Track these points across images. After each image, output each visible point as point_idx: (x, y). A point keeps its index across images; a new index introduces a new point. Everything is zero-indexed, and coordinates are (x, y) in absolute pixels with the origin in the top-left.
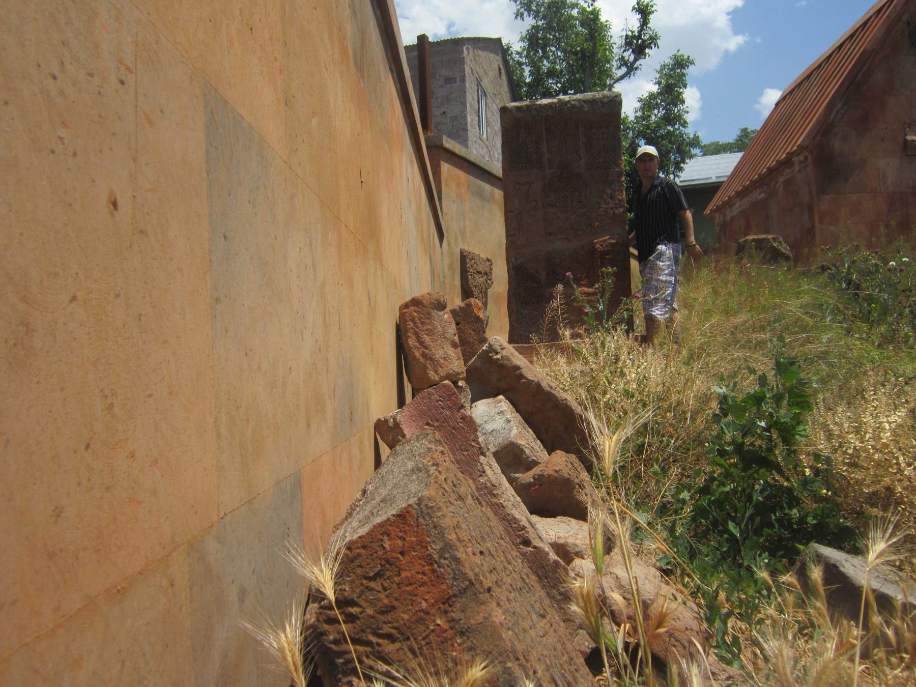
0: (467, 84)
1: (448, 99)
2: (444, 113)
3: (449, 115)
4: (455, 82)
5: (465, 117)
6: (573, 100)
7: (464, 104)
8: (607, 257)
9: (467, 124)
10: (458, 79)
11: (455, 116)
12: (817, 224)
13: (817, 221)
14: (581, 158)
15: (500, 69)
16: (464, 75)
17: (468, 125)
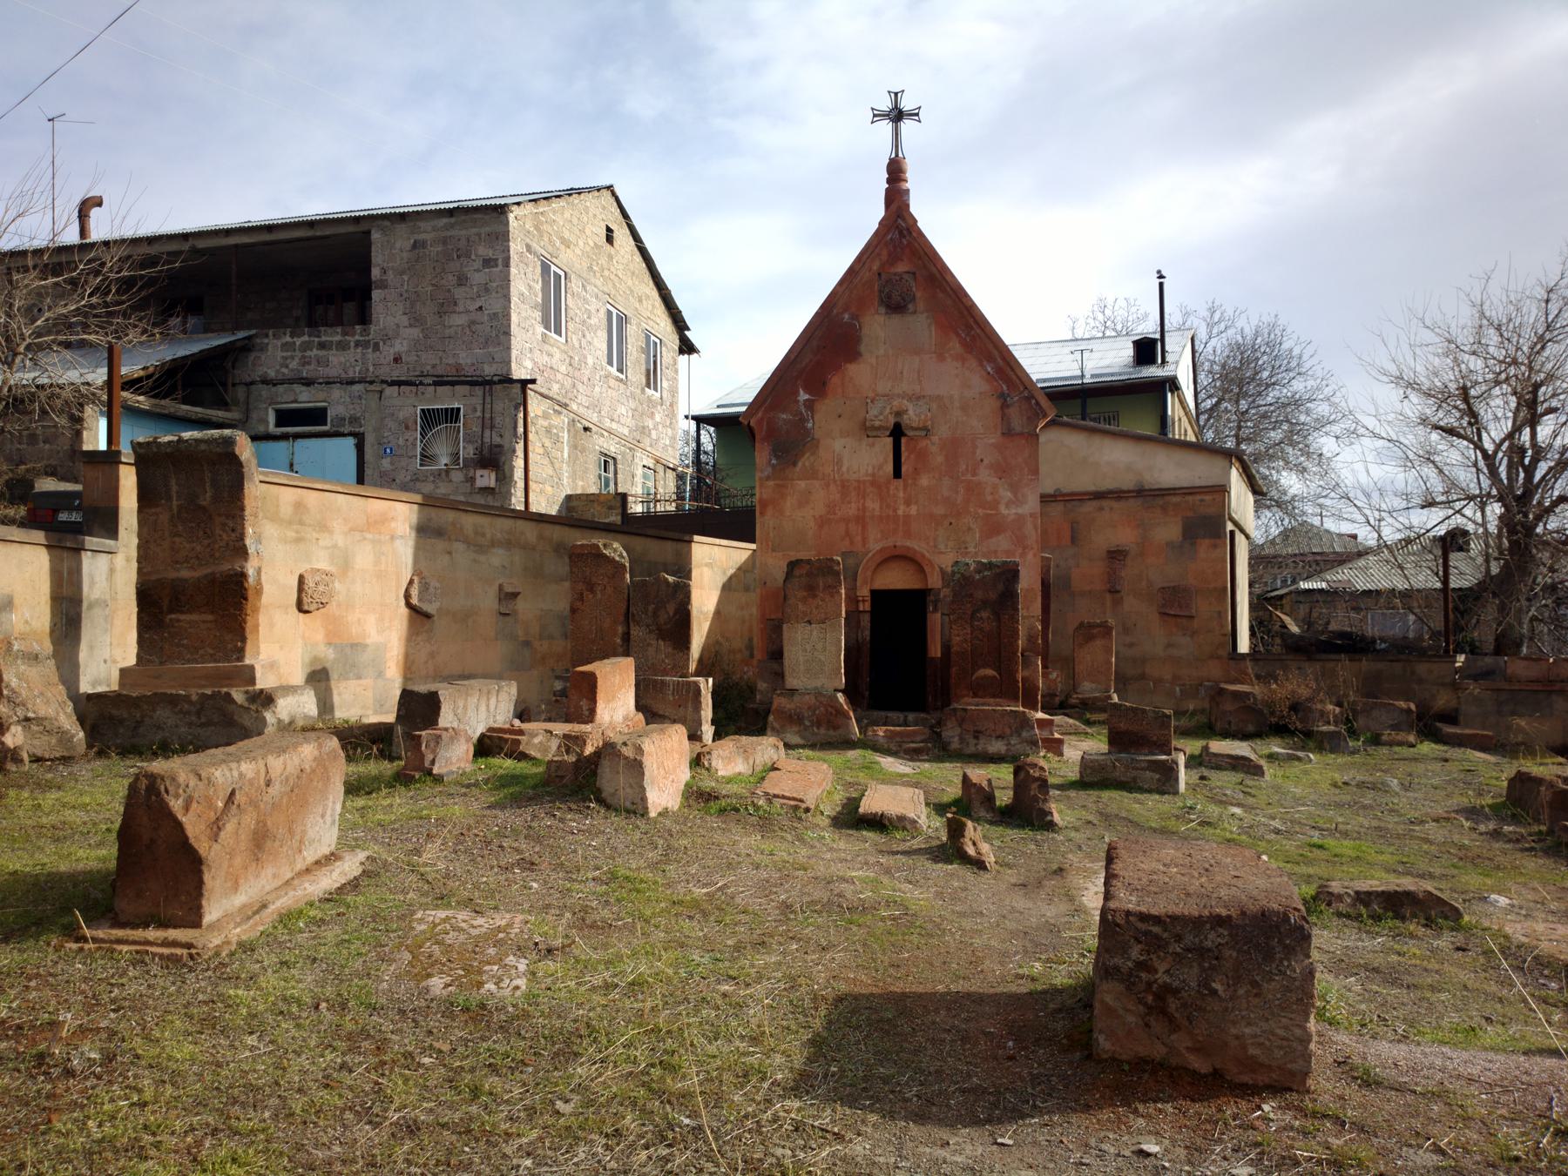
0: (513, 270)
2: (481, 308)
4: (497, 266)
5: (507, 316)
16: (509, 258)
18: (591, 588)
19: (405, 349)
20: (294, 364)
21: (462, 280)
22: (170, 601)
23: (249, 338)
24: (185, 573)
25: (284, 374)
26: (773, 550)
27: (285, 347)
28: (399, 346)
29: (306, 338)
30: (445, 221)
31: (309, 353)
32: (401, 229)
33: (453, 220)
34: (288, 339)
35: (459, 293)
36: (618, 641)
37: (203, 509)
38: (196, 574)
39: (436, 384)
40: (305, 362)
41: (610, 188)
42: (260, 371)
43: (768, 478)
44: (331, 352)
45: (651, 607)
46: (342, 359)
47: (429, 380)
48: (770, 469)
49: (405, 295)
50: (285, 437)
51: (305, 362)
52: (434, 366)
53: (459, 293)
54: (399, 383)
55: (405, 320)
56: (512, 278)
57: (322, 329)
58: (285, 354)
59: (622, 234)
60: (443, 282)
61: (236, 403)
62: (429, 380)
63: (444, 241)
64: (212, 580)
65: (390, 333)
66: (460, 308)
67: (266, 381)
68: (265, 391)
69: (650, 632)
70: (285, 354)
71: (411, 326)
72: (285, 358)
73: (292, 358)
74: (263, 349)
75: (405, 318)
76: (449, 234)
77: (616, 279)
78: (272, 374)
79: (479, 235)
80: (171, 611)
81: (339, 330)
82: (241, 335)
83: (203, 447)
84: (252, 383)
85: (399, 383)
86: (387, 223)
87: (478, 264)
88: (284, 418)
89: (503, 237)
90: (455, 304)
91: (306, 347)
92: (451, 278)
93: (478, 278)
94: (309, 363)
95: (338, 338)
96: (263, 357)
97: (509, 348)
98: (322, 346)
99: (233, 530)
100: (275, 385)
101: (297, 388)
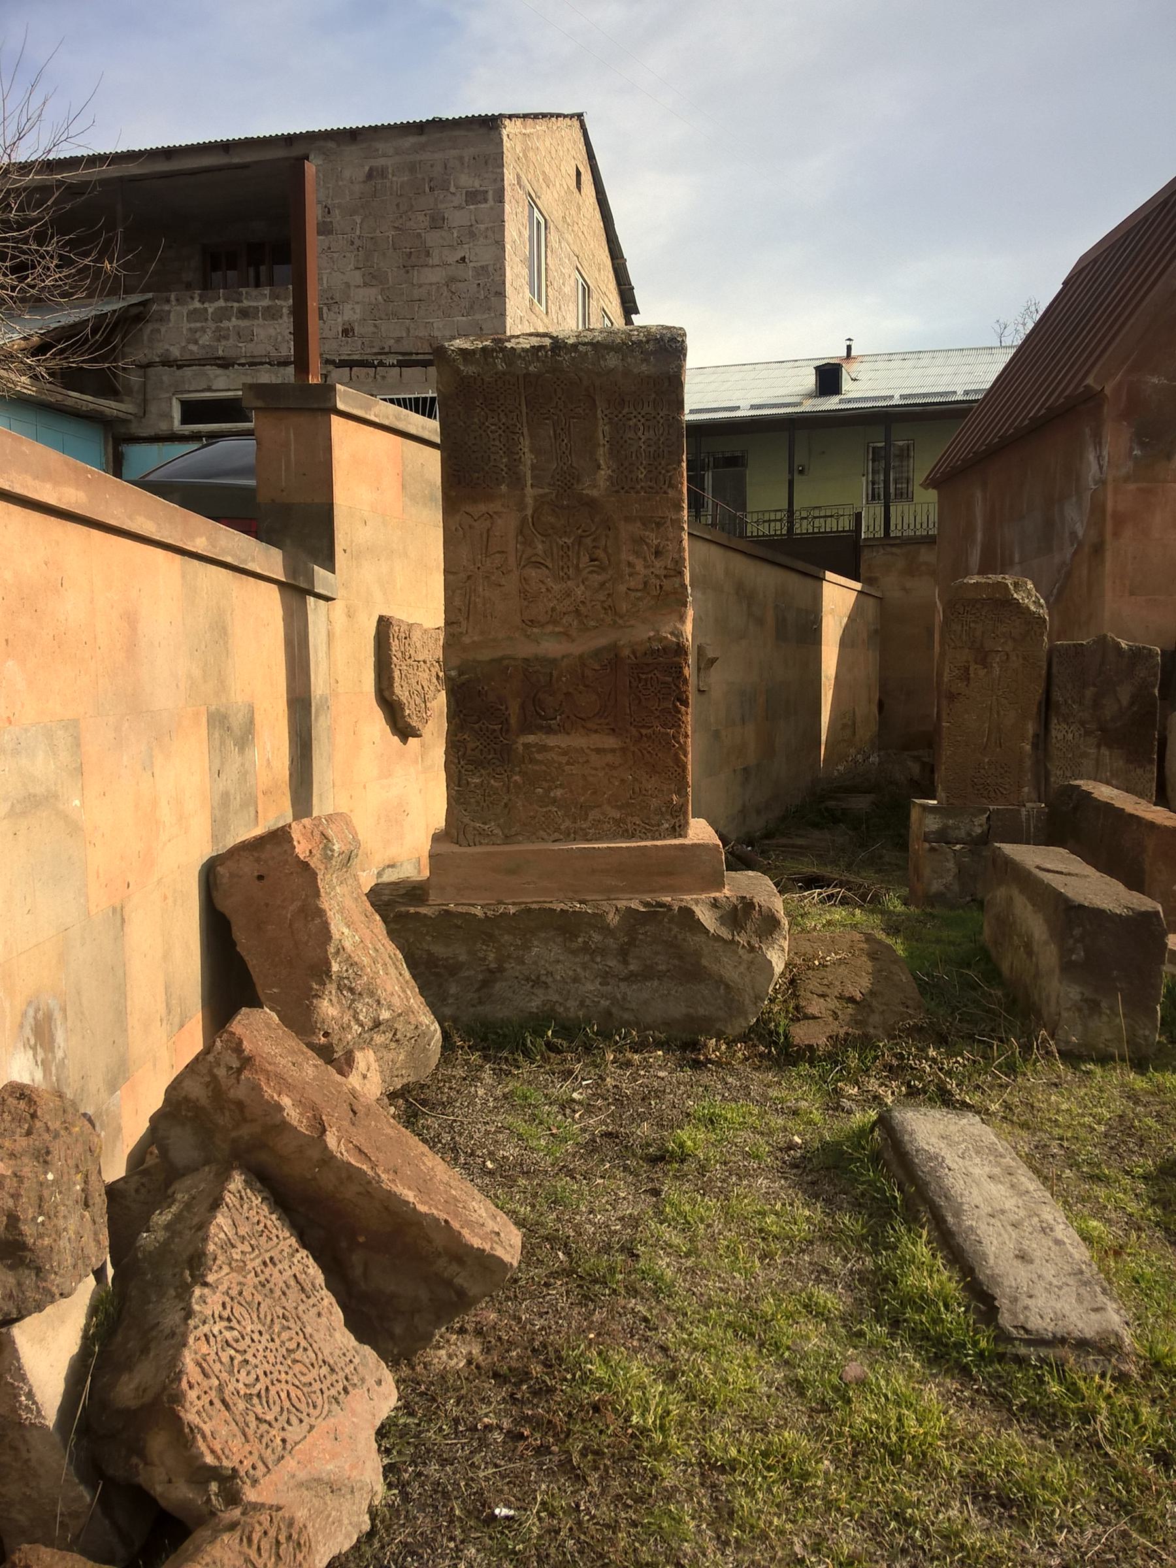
0: (507, 207)
1: (471, 233)
2: (463, 259)
3: (472, 264)
4: (486, 200)
6: (585, 344)
7: (500, 244)
8: (644, 676)
9: (504, 283)
10: (490, 195)
11: (482, 267)
12: (1108, 537)
13: (1109, 527)
14: (599, 467)
15: (578, 174)
16: (503, 189)
17: (507, 285)
18: (983, 657)
19: (357, 316)
20: (205, 339)
21: (437, 222)
22: (523, 707)
23: (143, 304)
24: (551, 647)
25: (192, 352)
26: (1132, 594)
27: (193, 315)
28: (350, 313)
29: (221, 303)
30: (411, 140)
31: (225, 324)
32: (352, 152)
33: (423, 139)
34: (197, 305)
35: (433, 239)
36: (1028, 747)
37: (591, 504)
38: (577, 648)
39: (401, 364)
40: (221, 336)
41: (580, 116)
42: (160, 348)
43: (1127, 479)
44: (256, 322)
45: (1090, 692)
46: (272, 332)
47: (392, 360)
48: (1130, 464)
49: (357, 243)
50: (195, 437)
51: (221, 336)
52: (399, 340)
53: (433, 239)
54: (350, 364)
55: (357, 277)
56: (506, 218)
57: (244, 290)
58: (192, 325)
59: (587, 177)
60: (412, 223)
61: (129, 392)
62: (392, 360)
63: (412, 168)
64: (612, 659)
65: (337, 298)
66: (435, 260)
67: (167, 363)
68: (166, 375)
69: (1088, 733)
70: (192, 325)
71: (366, 285)
72: (193, 331)
73: (203, 330)
74: (163, 318)
75: (358, 273)
76: (418, 157)
77: (582, 237)
78: (176, 352)
79: (461, 158)
80: (526, 728)
81: (267, 291)
82: (135, 299)
83: (612, 361)
84: (150, 365)
85: (350, 364)
86: (331, 145)
87: (459, 199)
88: (194, 411)
89: (496, 160)
90: (428, 254)
91: (223, 314)
92: (421, 218)
93: (458, 219)
94: (226, 338)
95: (266, 302)
96: (163, 330)
97: (503, 315)
98: (244, 314)
99: (658, 553)
100: (180, 367)
101: (212, 371)
